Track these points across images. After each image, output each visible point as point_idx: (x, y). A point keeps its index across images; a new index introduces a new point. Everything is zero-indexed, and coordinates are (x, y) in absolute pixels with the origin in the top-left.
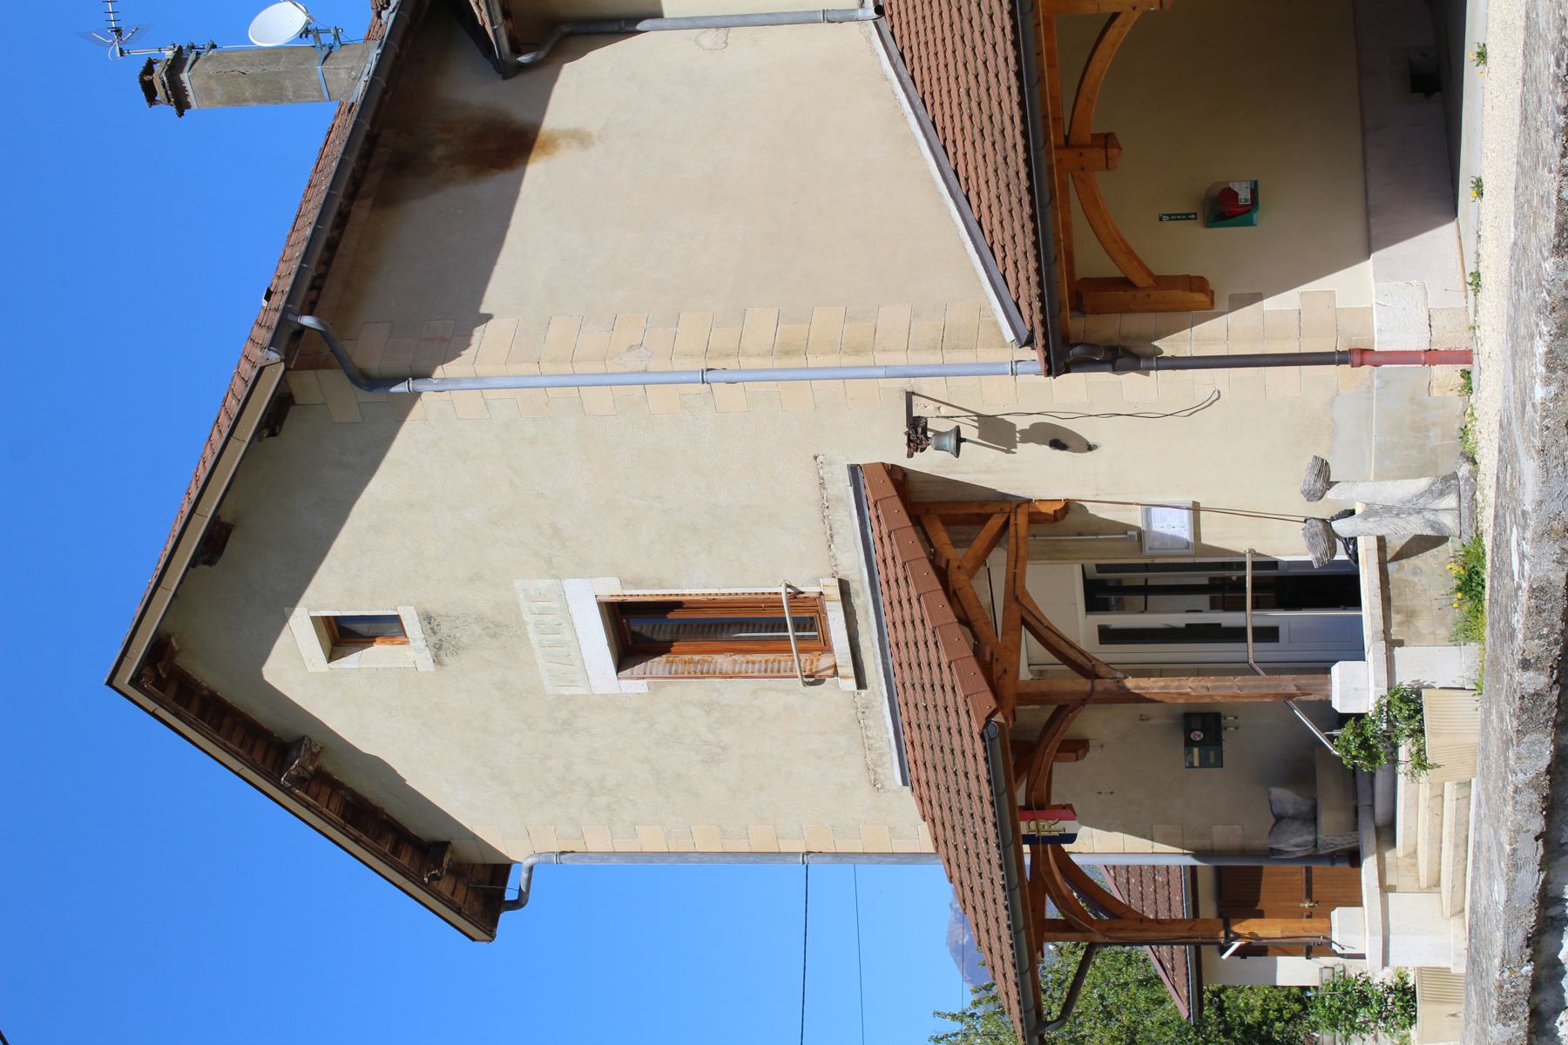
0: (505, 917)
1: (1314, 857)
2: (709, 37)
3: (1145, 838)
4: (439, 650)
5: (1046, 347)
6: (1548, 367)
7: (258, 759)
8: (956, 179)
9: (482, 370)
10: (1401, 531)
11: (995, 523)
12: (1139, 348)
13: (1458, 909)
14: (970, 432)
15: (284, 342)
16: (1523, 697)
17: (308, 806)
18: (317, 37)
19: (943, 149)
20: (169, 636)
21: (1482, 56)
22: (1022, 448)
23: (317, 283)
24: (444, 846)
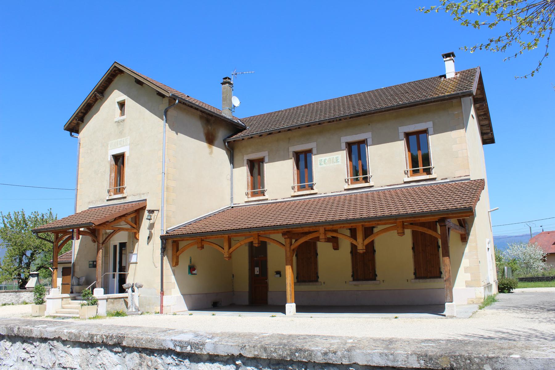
0: (69, 133)
1: (72, 285)
2: (229, 177)
3: (78, 253)
4: (118, 122)
5: (165, 236)
6: (69, 332)
7: (100, 88)
8: (200, 220)
9: (167, 132)
10: (129, 301)
11: (135, 226)
12: (165, 253)
13: (58, 312)
14: (152, 221)
15: (173, 97)
16: (13, 328)
17: (91, 97)
18: (233, 108)
19: (205, 218)
20: (124, 73)
21: (213, 315)
22: (148, 231)
23: (185, 104)
24: (83, 121)
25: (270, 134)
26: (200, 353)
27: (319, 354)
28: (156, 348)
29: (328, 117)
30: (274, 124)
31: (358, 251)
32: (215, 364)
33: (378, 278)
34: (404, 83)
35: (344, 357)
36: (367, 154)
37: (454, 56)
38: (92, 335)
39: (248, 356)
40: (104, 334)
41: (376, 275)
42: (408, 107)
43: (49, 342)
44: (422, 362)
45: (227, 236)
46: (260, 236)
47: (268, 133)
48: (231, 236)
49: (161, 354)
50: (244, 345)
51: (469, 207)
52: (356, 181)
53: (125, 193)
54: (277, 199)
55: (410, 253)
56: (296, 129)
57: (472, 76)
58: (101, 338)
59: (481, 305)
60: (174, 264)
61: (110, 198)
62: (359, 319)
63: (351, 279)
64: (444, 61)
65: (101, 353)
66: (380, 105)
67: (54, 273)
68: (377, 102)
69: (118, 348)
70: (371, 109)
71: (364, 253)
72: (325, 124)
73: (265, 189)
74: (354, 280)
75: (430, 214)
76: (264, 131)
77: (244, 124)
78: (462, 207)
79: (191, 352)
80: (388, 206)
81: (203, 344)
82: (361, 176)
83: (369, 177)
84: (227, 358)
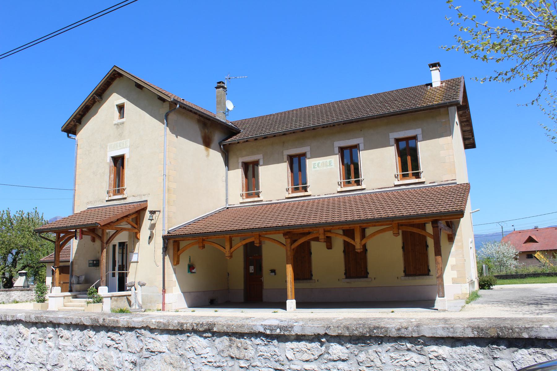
0: (66, 134)
1: (71, 284)
2: (224, 178)
4: (117, 125)
5: (167, 236)
7: (99, 91)
8: (198, 220)
10: (132, 299)
11: (136, 226)
14: (153, 222)
17: (89, 99)
18: (227, 112)
19: (203, 218)
21: (216, 311)
22: (149, 231)
24: (80, 123)
25: (265, 138)
26: (289, 334)
27: (394, 330)
28: (246, 332)
29: (322, 123)
30: (267, 127)
31: (356, 250)
32: (302, 342)
33: (369, 276)
34: (392, 90)
35: (414, 331)
36: (359, 158)
37: (439, 65)
38: (181, 323)
39: (333, 334)
40: (194, 322)
41: (368, 273)
42: (398, 114)
43: (136, 330)
44: (476, 333)
45: (228, 236)
46: (261, 236)
47: (264, 137)
48: (233, 236)
49: (251, 336)
50: (329, 326)
51: (460, 210)
52: (348, 184)
53: (125, 194)
54: (271, 201)
55: (400, 252)
56: (291, 133)
57: (458, 86)
58: (192, 325)
59: (467, 300)
60: (175, 263)
61: (110, 199)
62: (359, 314)
63: (344, 277)
64: (431, 71)
65: (190, 339)
66: (372, 112)
67: (56, 272)
68: (368, 109)
69: (208, 333)
70: (363, 116)
71: (361, 252)
72: (319, 129)
73: (260, 191)
74: (347, 278)
75: (424, 216)
76: (259, 135)
77: (237, 127)
78: (454, 210)
79: (280, 333)
80: (383, 208)
81: (292, 327)
82: (353, 180)
83: (361, 180)
84: (312, 337)
